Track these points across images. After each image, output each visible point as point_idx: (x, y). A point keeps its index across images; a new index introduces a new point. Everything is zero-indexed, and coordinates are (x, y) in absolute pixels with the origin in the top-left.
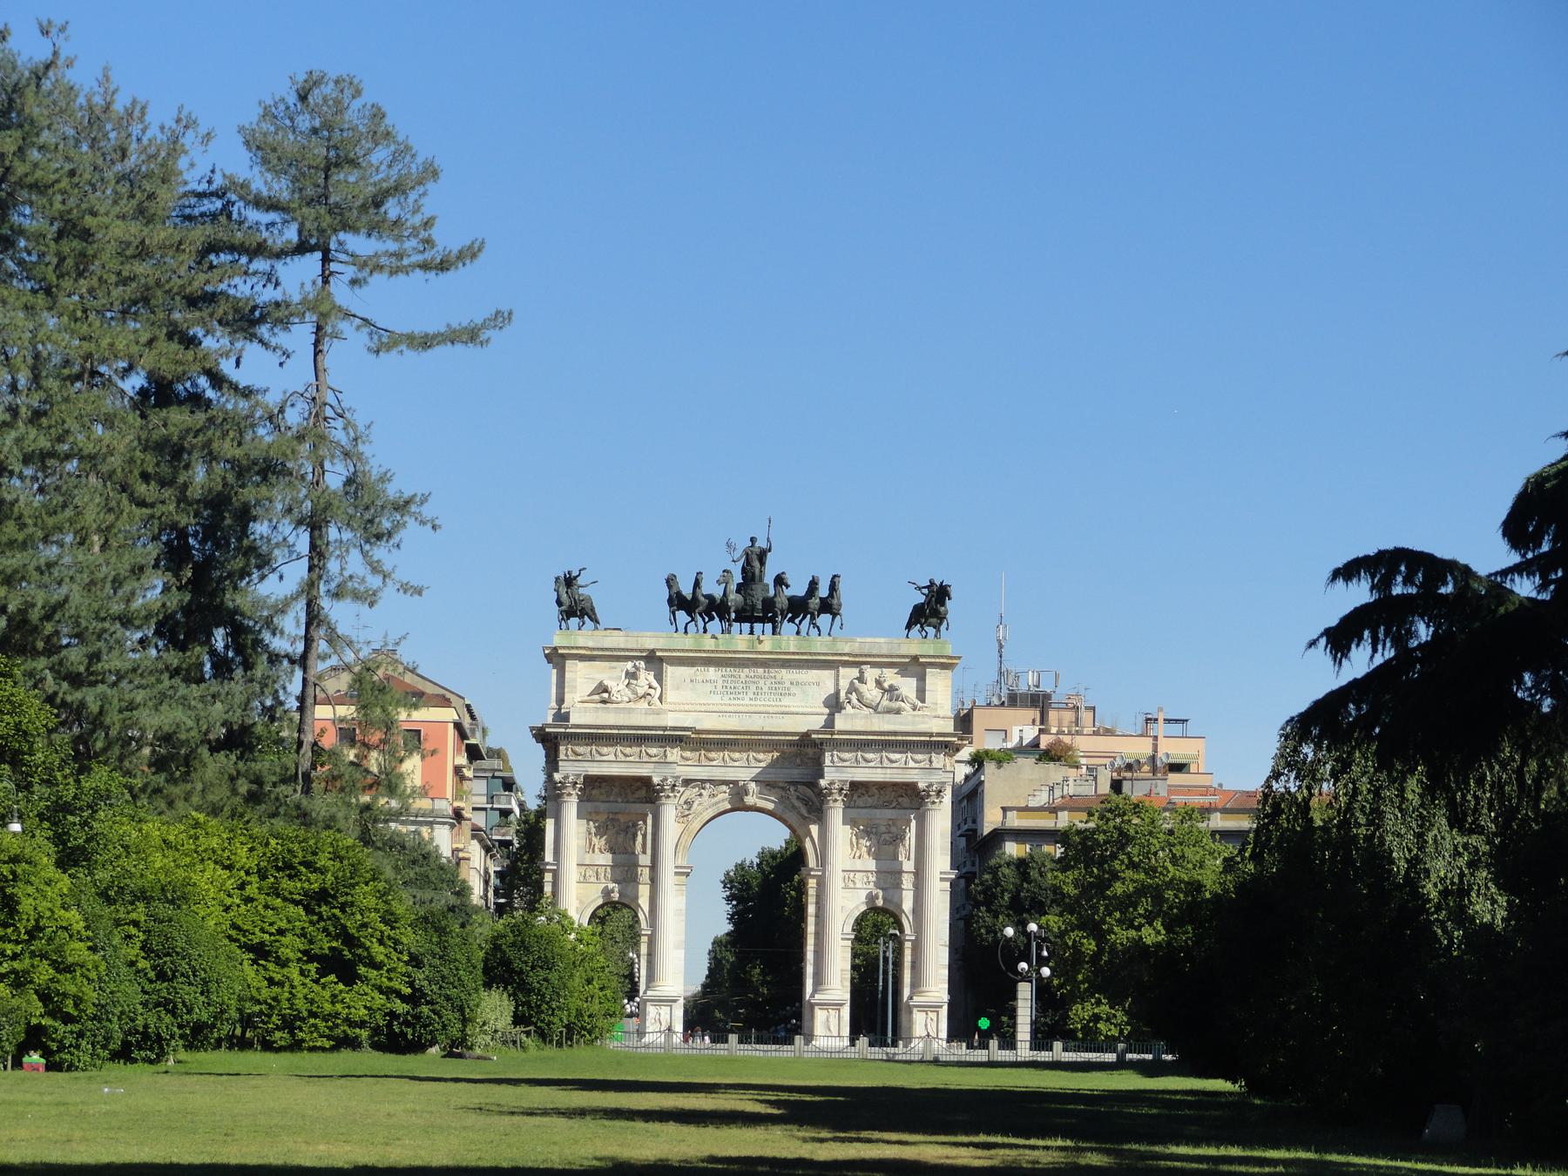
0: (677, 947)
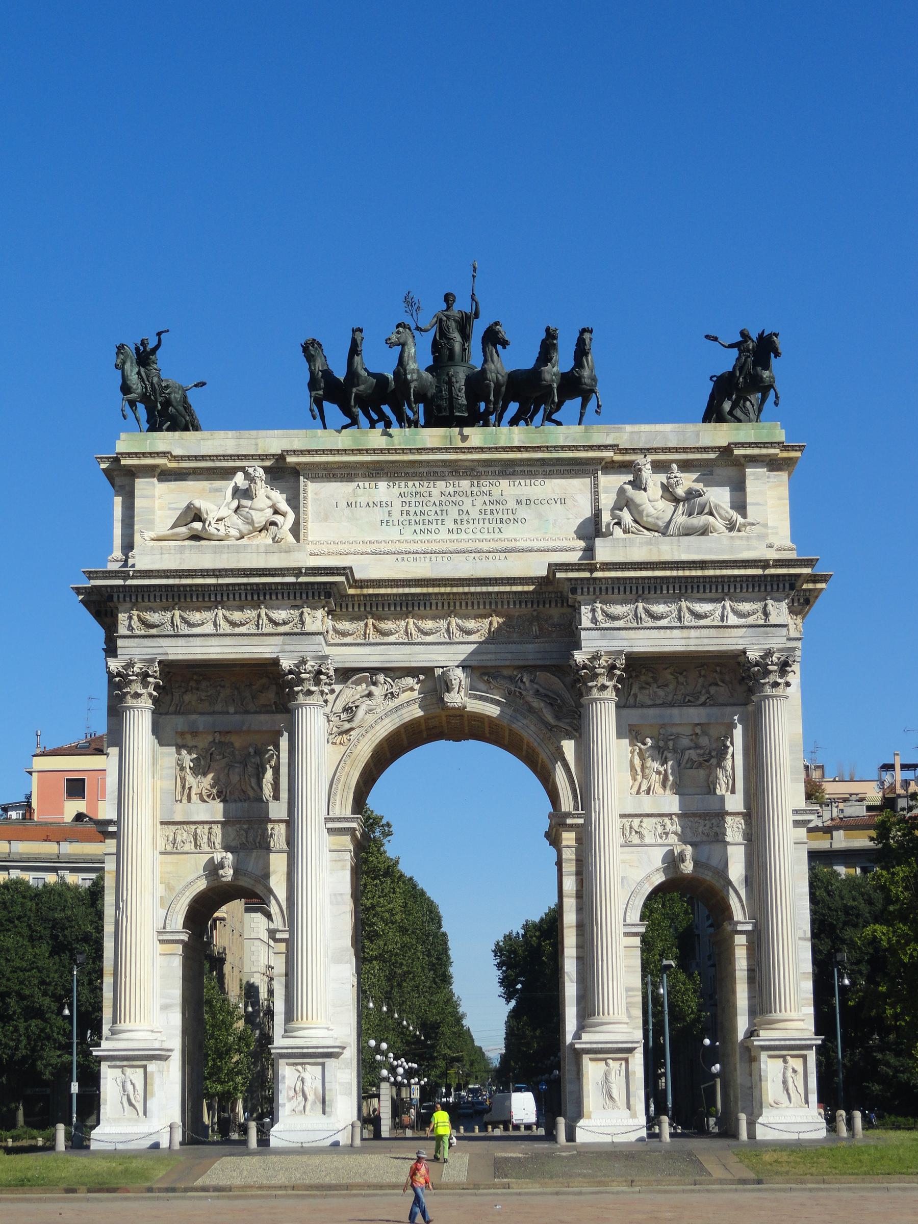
0: (337, 959)
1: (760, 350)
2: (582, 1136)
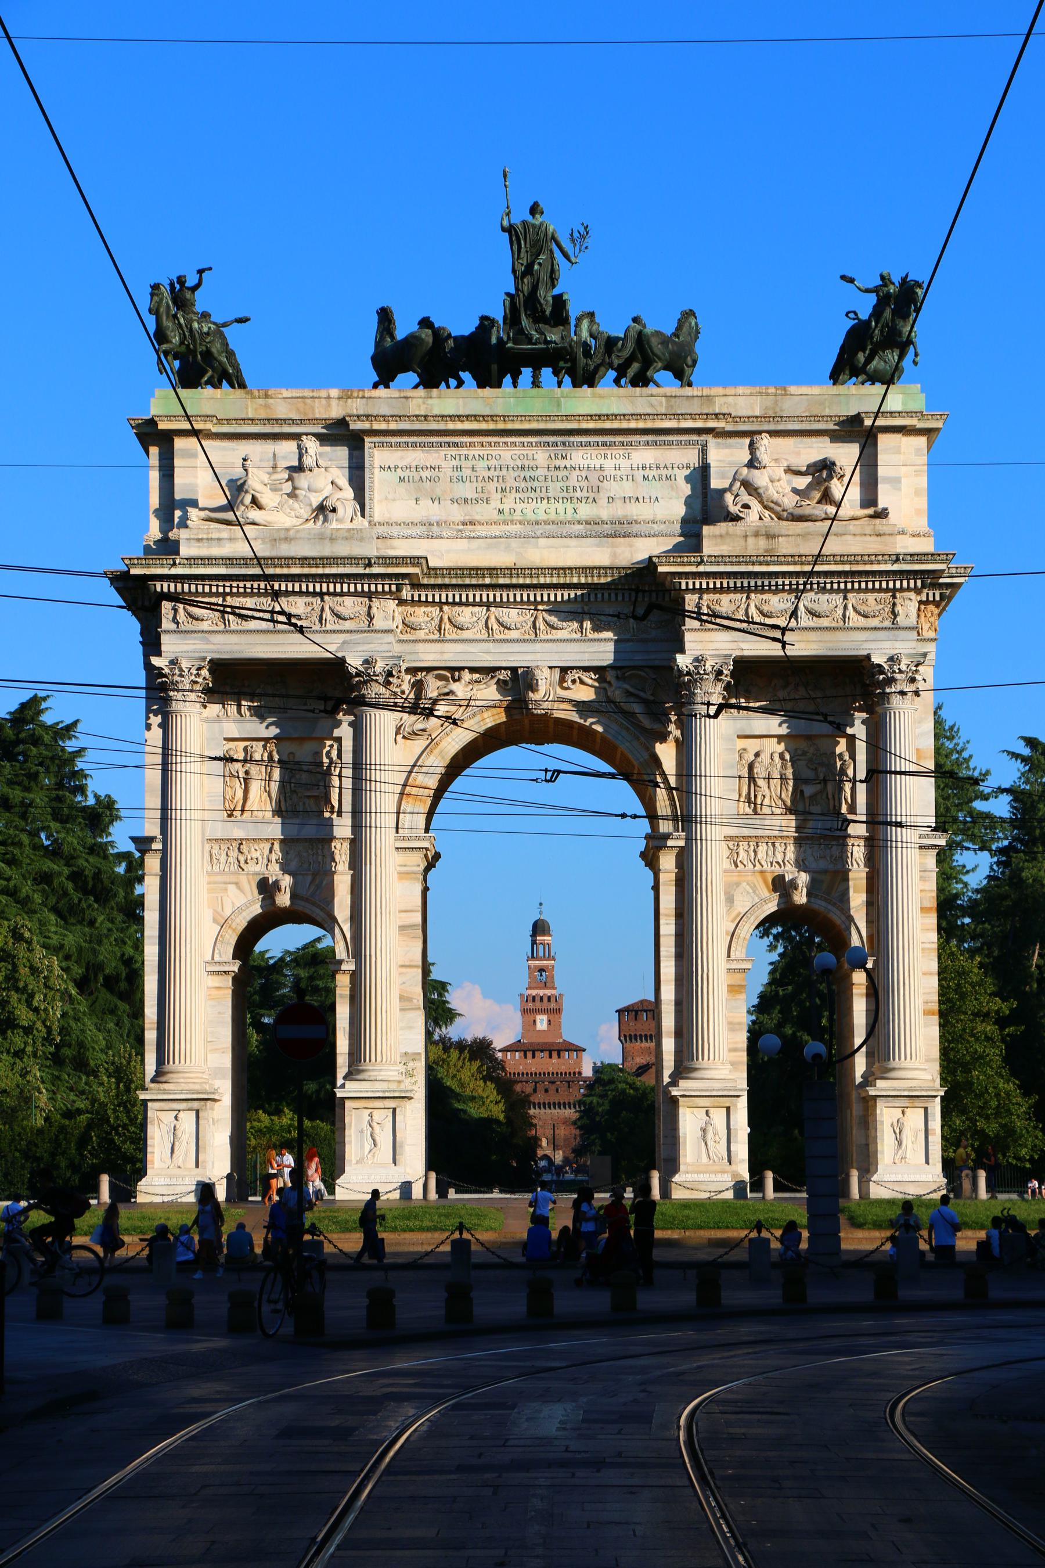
1: (900, 301)
2: (677, 1194)
